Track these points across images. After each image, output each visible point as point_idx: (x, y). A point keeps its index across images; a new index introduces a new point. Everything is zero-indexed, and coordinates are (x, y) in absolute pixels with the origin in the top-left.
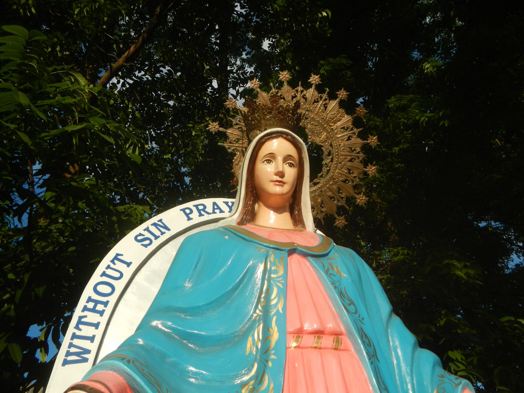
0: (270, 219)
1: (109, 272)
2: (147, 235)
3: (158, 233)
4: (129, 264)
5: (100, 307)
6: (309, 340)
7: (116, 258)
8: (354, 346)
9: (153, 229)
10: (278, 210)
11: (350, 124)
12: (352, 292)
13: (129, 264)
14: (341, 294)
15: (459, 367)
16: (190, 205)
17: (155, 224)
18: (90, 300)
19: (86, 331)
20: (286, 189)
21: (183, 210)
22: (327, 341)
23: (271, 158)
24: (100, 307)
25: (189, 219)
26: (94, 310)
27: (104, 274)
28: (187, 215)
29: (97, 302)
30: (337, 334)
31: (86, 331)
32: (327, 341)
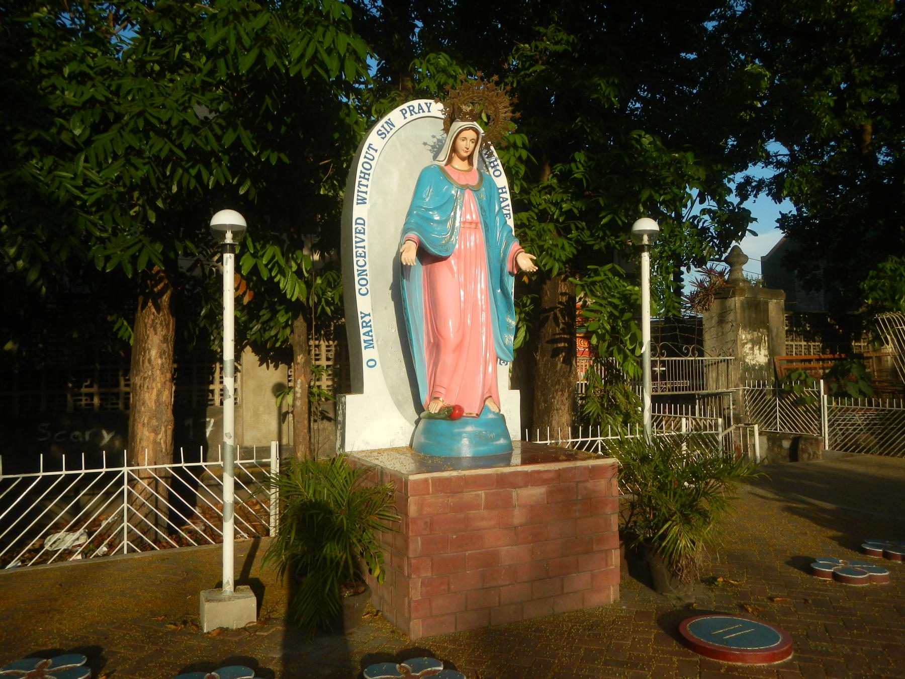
0: (458, 164)
1: (368, 156)
2: (383, 131)
3: (389, 129)
4: (376, 151)
5: (367, 176)
6: (467, 225)
7: (369, 147)
8: (481, 227)
9: (386, 126)
10: (463, 159)
11: (507, 104)
12: (485, 207)
13: (376, 151)
14: (481, 208)
15: (578, 168)
16: (405, 106)
17: (386, 123)
18: (361, 172)
19: (363, 189)
20: (469, 154)
21: (401, 111)
22: (473, 226)
23: (465, 139)
24: (367, 176)
25: (405, 118)
26: (364, 178)
27: (365, 157)
28: (404, 115)
29: (365, 174)
30: (477, 224)
31: (363, 189)
32: (473, 226)
